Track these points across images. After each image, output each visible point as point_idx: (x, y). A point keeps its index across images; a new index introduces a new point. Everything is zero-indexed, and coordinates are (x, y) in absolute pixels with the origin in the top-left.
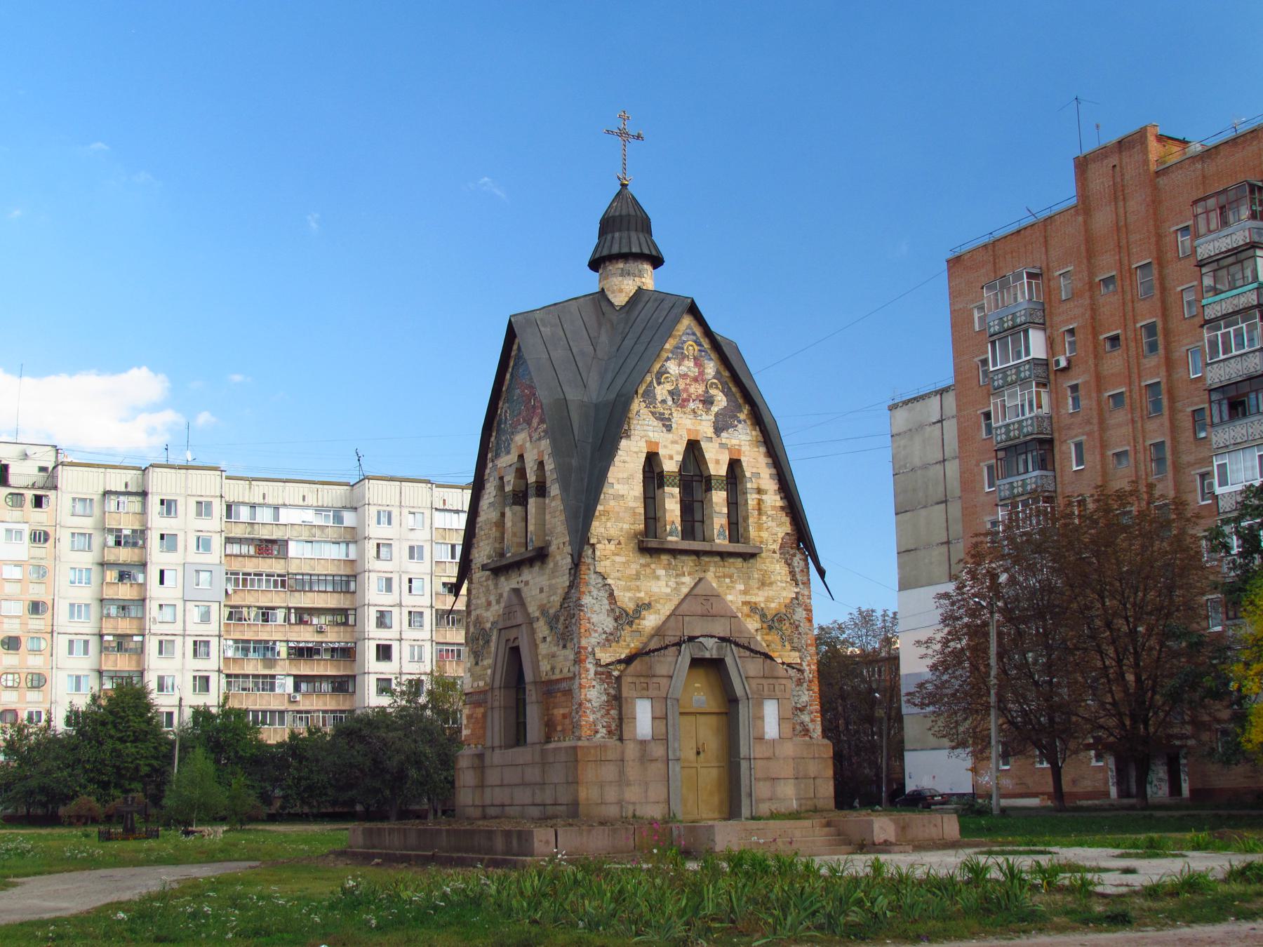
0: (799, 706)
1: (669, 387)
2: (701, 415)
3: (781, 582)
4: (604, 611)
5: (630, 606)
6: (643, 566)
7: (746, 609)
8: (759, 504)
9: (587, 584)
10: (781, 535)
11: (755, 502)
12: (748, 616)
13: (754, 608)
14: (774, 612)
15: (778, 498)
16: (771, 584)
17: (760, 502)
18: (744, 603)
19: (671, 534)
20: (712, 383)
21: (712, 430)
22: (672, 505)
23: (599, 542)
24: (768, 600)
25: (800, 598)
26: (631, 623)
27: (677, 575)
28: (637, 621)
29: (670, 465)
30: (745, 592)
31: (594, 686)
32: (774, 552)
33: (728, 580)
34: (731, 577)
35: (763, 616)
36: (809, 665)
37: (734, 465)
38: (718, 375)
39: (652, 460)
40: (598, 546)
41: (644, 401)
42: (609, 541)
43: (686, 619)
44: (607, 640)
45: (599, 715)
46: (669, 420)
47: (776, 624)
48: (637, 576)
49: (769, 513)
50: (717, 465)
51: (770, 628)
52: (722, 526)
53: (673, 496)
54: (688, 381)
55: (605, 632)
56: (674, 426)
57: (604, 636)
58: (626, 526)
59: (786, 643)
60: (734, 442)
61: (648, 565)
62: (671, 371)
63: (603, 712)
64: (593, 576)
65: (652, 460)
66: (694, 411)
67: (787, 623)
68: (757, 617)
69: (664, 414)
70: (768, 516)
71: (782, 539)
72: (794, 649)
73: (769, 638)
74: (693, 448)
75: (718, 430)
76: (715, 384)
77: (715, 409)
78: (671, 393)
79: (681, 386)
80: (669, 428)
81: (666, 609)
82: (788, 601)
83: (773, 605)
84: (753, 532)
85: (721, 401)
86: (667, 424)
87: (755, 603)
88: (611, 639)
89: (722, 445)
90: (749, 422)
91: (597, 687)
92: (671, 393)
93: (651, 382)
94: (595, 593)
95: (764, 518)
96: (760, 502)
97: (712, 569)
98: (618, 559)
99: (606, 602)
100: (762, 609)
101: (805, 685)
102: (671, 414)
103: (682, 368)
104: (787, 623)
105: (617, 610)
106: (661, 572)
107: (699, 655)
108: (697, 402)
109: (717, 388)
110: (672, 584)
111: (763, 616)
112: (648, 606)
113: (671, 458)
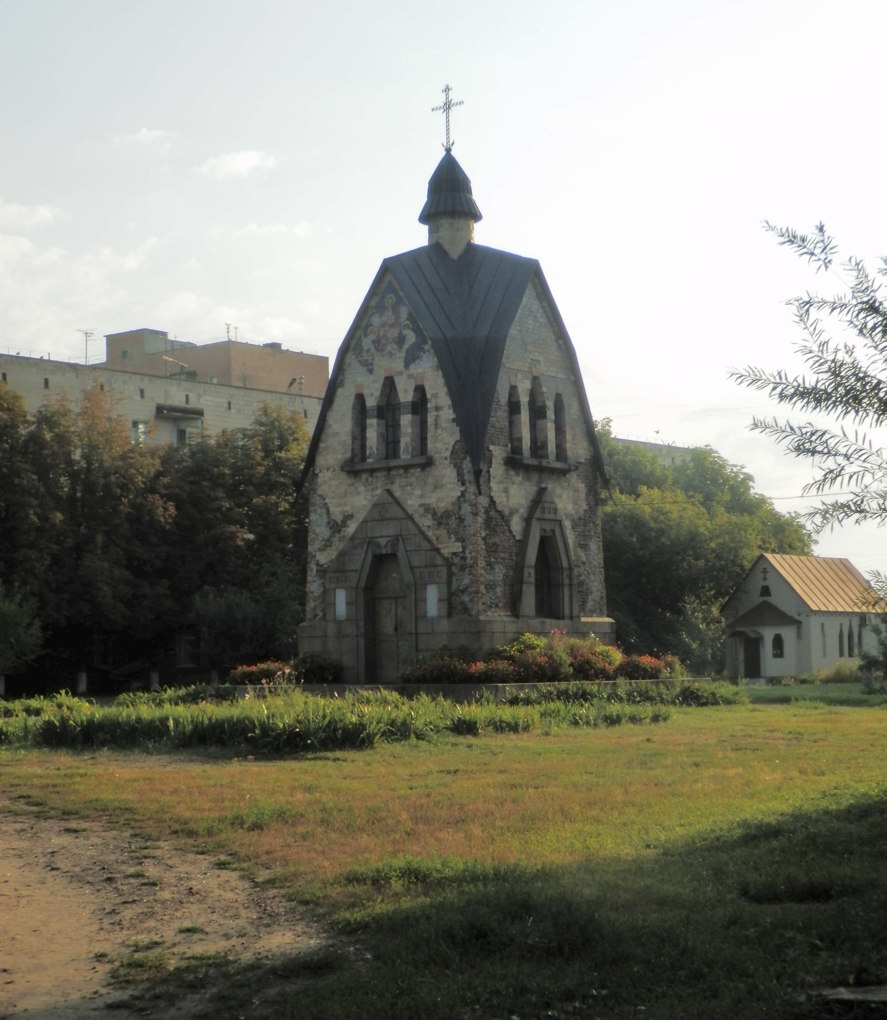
0: (461, 588)
1: (373, 337)
2: (395, 355)
3: (450, 484)
4: (324, 524)
5: (339, 518)
6: (350, 485)
7: (421, 510)
8: (436, 420)
9: (315, 505)
10: (452, 443)
11: (434, 418)
12: (423, 516)
13: (427, 509)
14: (442, 510)
15: (451, 411)
16: (442, 486)
17: (437, 418)
18: (420, 506)
19: (369, 457)
20: (405, 325)
21: (403, 365)
22: (372, 435)
23: (321, 472)
24: (439, 500)
25: (467, 495)
26: (339, 532)
27: (373, 489)
28: (344, 529)
29: (371, 402)
30: (421, 497)
31: (315, 581)
32: (446, 459)
33: (409, 488)
34: (411, 485)
35: (434, 514)
36: (470, 553)
37: (420, 390)
38: (410, 317)
39: (360, 399)
40: (320, 475)
41: (355, 354)
42: (328, 470)
43: (369, 524)
44: (326, 546)
45: (317, 603)
46: (372, 364)
47: (445, 521)
48: (345, 495)
49: (444, 426)
50: (406, 395)
51: (440, 524)
52: (406, 444)
53: (372, 425)
54: (387, 329)
55: (324, 540)
56: (375, 368)
57: (323, 543)
58: (339, 456)
59: (452, 536)
60: (420, 370)
61: (353, 484)
62: (374, 323)
63: (320, 600)
64: (318, 498)
65: (360, 399)
66: (390, 353)
67: (453, 518)
68: (430, 516)
69: (367, 360)
70: (443, 429)
71: (454, 446)
72: (458, 540)
73: (438, 532)
74: (389, 384)
75: (407, 366)
76: (408, 325)
77: (406, 347)
78: (374, 342)
79: (381, 334)
80: (371, 371)
81: (360, 517)
82: (455, 499)
83: (442, 505)
84: (430, 445)
85: (411, 338)
86: (369, 368)
87: (429, 505)
88: (328, 544)
89: (410, 376)
90: (432, 351)
91: (318, 582)
92: (374, 342)
93: (360, 336)
94: (319, 511)
95: (439, 431)
96: (437, 418)
97: (398, 481)
98: (334, 483)
99: (325, 516)
100: (434, 509)
101: (467, 570)
102: (373, 359)
103: (384, 318)
104: (453, 518)
105: (332, 522)
106: (362, 489)
107: (378, 552)
108: (393, 344)
109: (409, 327)
110: (369, 497)
111: (434, 514)
112: (351, 517)
113: (372, 395)
